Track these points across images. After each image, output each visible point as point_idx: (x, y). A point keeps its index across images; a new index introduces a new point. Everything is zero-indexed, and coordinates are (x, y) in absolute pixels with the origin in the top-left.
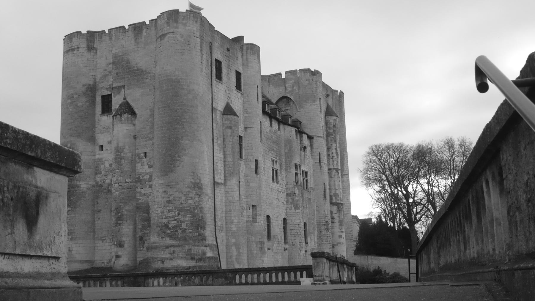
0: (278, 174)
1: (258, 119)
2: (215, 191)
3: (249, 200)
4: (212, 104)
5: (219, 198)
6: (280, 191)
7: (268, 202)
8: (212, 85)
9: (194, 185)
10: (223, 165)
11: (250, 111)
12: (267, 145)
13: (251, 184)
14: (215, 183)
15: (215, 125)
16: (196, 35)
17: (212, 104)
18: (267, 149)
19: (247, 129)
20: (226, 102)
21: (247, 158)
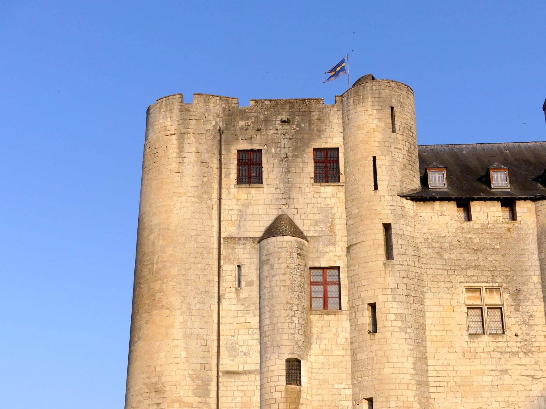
0: (506, 313)
1: (377, 221)
2: (221, 388)
3: (357, 390)
4: (220, 233)
5: (239, 400)
6: (515, 350)
7: (441, 384)
8: (220, 200)
9: (149, 389)
10: (258, 337)
11: (357, 211)
12: (440, 261)
13: (360, 356)
14: (220, 374)
15: (229, 270)
16: (169, 133)
17: (220, 233)
18: (440, 272)
19: (352, 248)
20: (273, 217)
21: (353, 307)
